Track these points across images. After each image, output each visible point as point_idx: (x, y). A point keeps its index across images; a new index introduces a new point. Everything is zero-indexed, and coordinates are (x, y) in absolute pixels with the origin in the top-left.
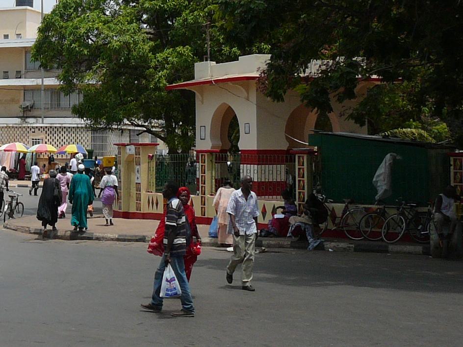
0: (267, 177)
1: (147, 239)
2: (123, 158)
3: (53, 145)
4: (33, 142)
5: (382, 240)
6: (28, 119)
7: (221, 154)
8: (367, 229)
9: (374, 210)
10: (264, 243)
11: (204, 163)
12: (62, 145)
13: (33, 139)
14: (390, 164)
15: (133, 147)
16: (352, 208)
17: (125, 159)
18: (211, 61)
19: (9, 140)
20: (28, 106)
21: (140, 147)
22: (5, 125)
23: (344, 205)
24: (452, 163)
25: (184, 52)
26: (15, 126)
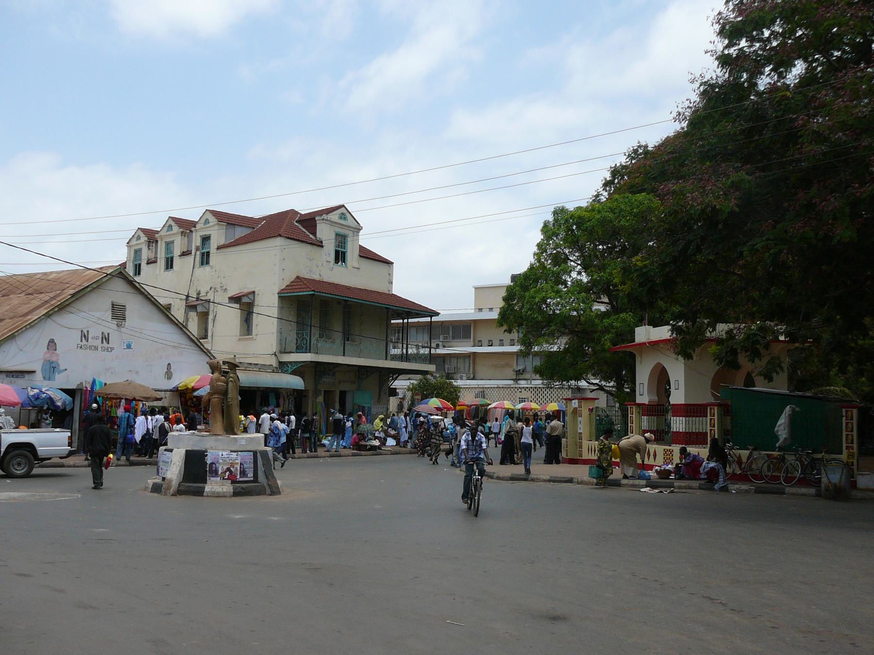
0: (691, 427)
1: (574, 480)
2: (569, 411)
3: (537, 404)
4: (520, 400)
5: (781, 483)
6: (520, 381)
7: (659, 407)
8: (768, 474)
9: (776, 456)
10: (675, 484)
11: (633, 414)
12: (545, 403)
13: (520, 398)
14: (789, 415)
15: (576, 401)
16: (756, 454)
17: (571, 412)
18: (648, 325)
19: (500, 399)
20: (520, 370)
21: (582, 401)
22: (496, 386)
23: (749, 451)
24: (844, 414)
25: (627, 318)
26: (504, 386)
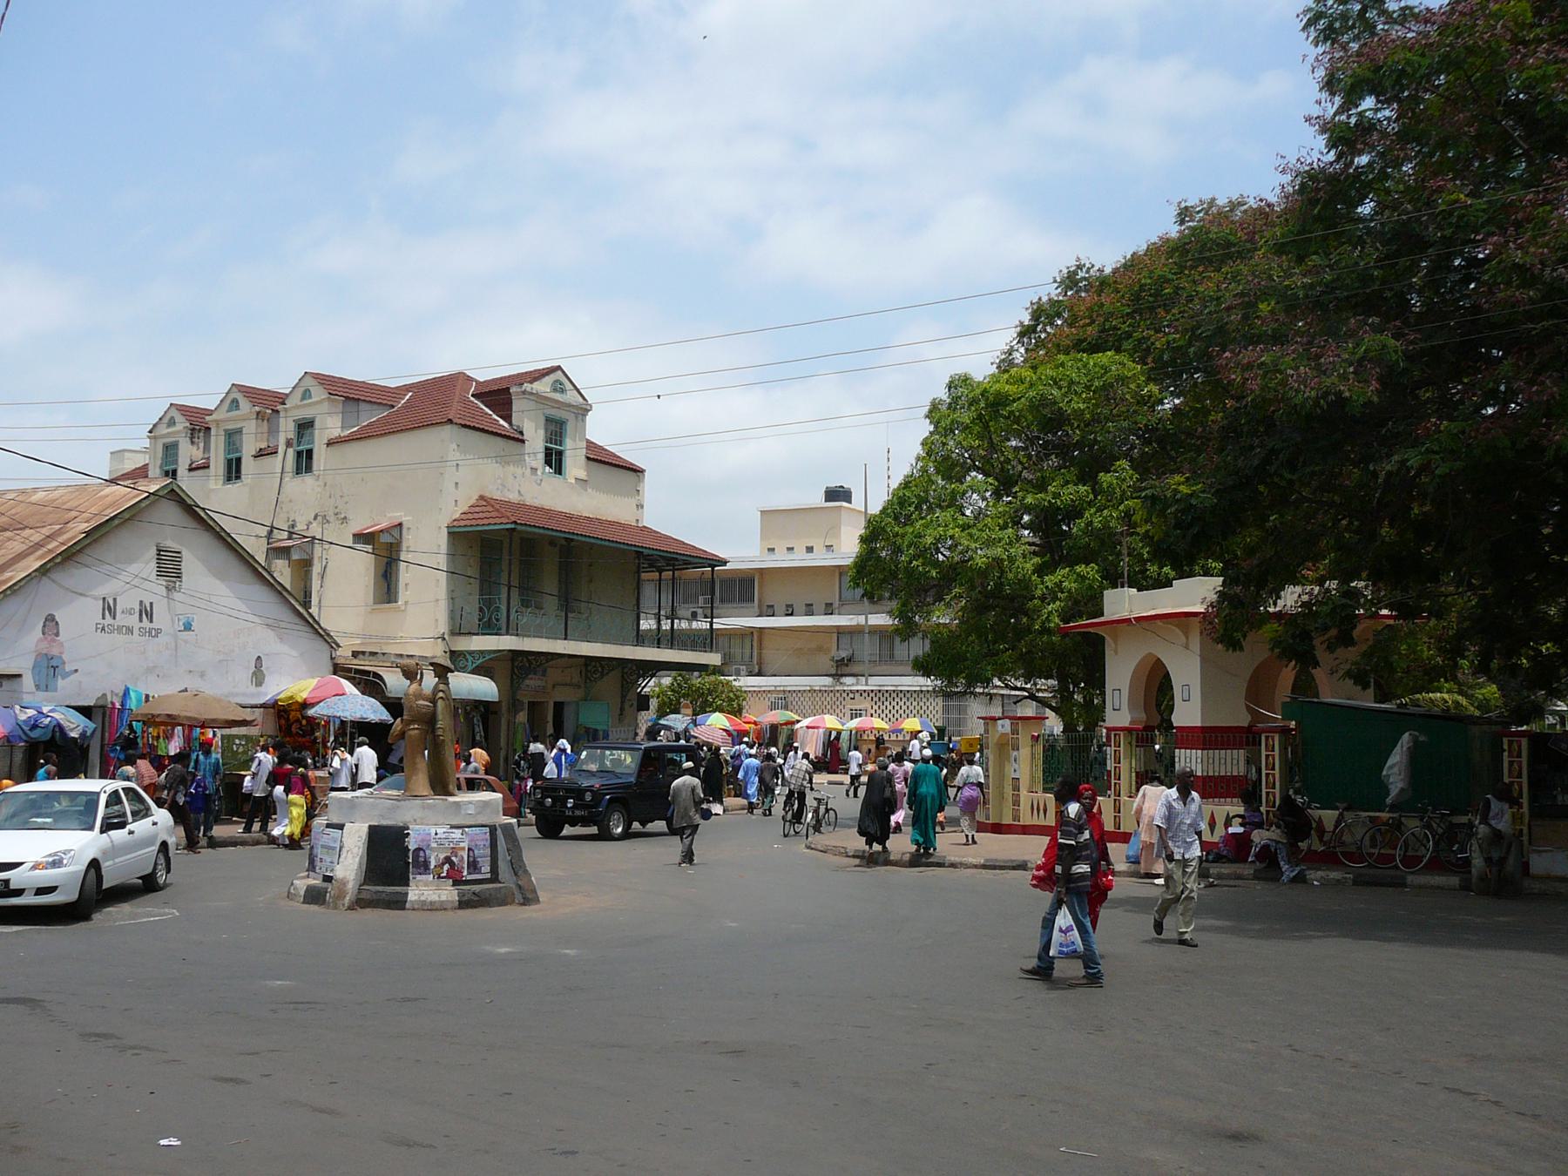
1: (1029, 865)
2: (993, 740)
5: (1397, 867)
8: (1373, 851)
9: (1385, 820)
14: (1409, 748)
15: (1007, 722)
16: (1350, 817)
17: (995, 741)
18: (1129, 587)
22: (808, 688)
23: (1337, 812)
24: (1506, 747)
25: (1088, 573)
